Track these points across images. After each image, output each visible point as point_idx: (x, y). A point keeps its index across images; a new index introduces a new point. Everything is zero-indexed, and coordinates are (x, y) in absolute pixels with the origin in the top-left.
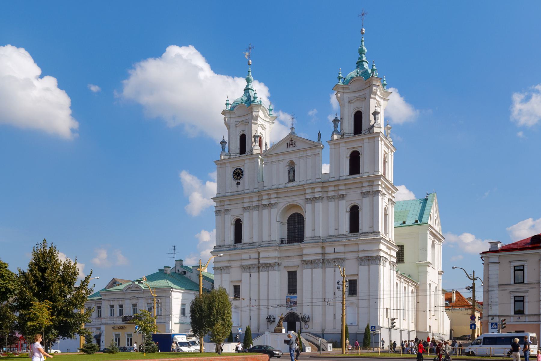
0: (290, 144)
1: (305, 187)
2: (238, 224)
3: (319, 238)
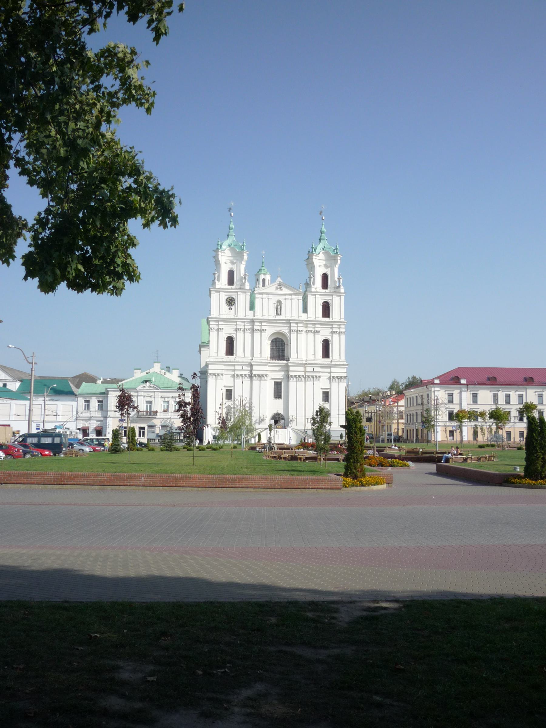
1: (291, 322)
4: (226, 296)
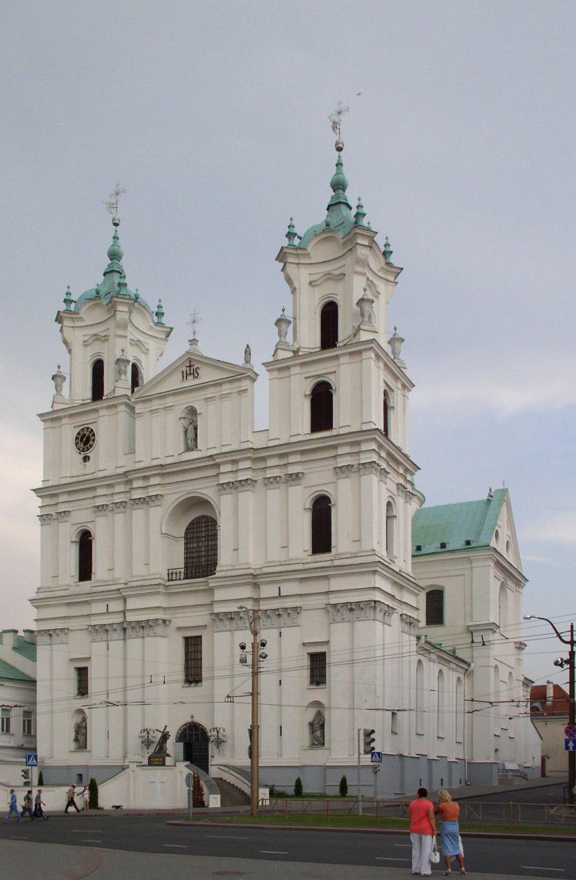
0: (188, 373)
2: (85, 542)
4: (75, 427)
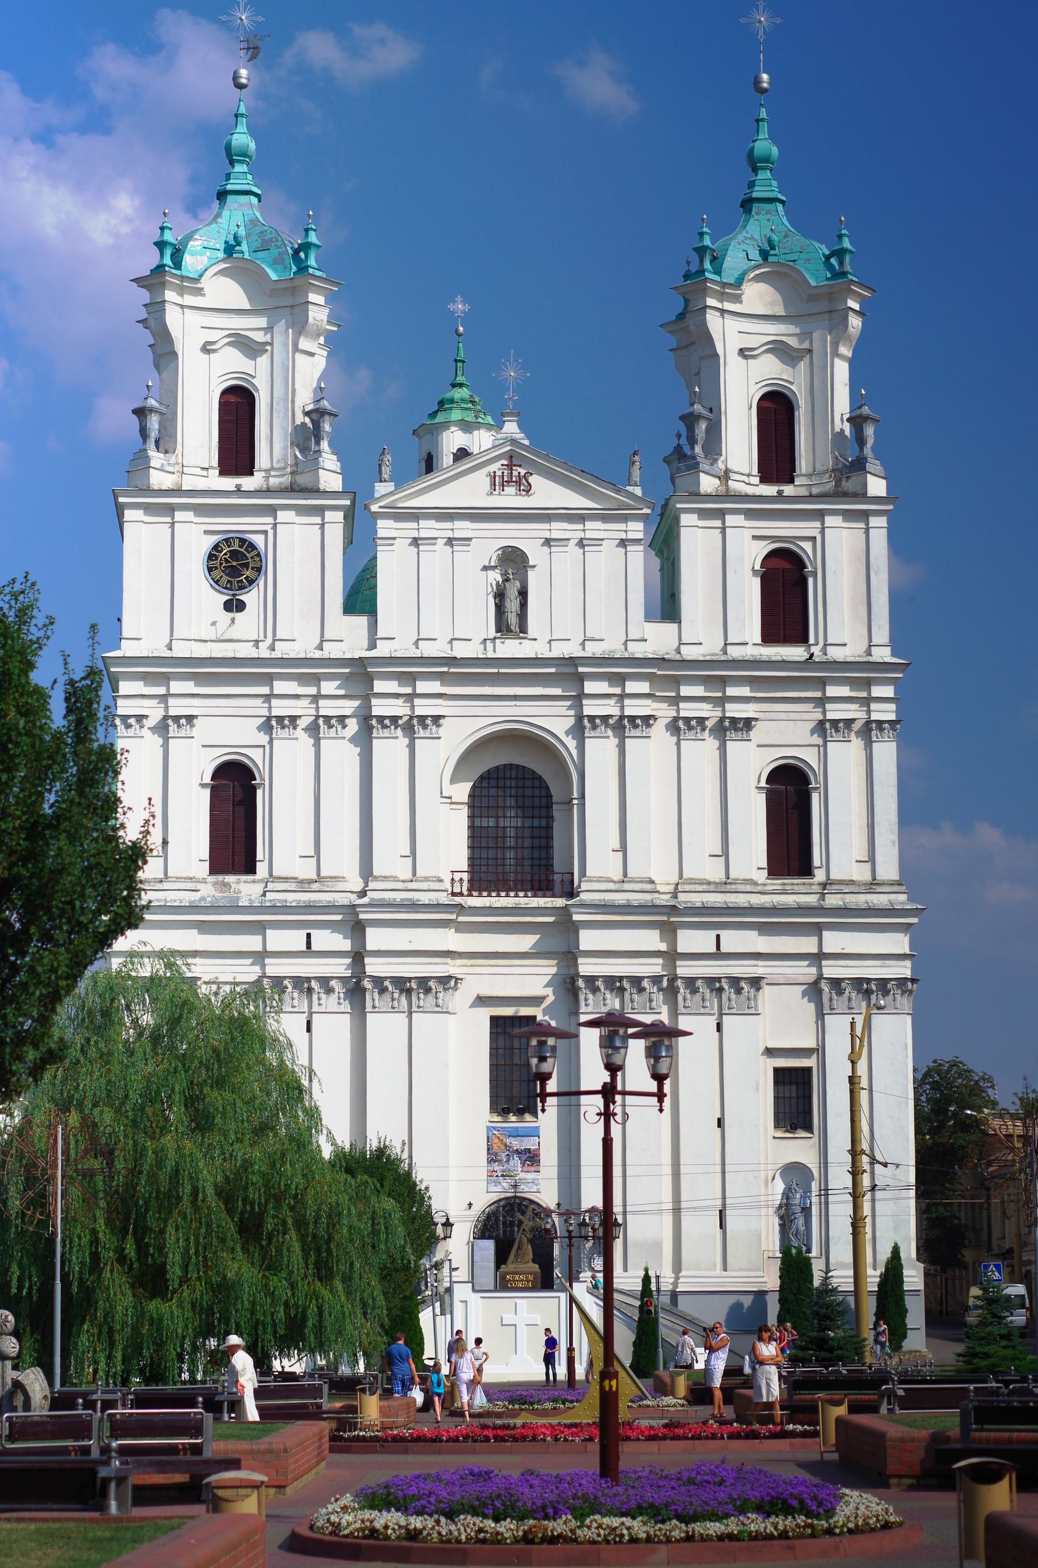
1: (581, 669)
3: (649, 887)
4: (206, 532)
